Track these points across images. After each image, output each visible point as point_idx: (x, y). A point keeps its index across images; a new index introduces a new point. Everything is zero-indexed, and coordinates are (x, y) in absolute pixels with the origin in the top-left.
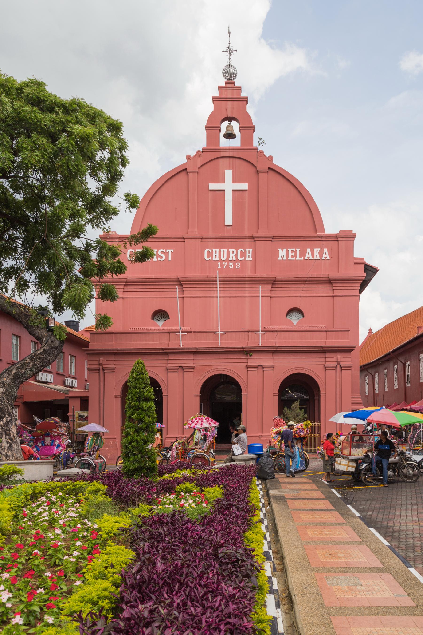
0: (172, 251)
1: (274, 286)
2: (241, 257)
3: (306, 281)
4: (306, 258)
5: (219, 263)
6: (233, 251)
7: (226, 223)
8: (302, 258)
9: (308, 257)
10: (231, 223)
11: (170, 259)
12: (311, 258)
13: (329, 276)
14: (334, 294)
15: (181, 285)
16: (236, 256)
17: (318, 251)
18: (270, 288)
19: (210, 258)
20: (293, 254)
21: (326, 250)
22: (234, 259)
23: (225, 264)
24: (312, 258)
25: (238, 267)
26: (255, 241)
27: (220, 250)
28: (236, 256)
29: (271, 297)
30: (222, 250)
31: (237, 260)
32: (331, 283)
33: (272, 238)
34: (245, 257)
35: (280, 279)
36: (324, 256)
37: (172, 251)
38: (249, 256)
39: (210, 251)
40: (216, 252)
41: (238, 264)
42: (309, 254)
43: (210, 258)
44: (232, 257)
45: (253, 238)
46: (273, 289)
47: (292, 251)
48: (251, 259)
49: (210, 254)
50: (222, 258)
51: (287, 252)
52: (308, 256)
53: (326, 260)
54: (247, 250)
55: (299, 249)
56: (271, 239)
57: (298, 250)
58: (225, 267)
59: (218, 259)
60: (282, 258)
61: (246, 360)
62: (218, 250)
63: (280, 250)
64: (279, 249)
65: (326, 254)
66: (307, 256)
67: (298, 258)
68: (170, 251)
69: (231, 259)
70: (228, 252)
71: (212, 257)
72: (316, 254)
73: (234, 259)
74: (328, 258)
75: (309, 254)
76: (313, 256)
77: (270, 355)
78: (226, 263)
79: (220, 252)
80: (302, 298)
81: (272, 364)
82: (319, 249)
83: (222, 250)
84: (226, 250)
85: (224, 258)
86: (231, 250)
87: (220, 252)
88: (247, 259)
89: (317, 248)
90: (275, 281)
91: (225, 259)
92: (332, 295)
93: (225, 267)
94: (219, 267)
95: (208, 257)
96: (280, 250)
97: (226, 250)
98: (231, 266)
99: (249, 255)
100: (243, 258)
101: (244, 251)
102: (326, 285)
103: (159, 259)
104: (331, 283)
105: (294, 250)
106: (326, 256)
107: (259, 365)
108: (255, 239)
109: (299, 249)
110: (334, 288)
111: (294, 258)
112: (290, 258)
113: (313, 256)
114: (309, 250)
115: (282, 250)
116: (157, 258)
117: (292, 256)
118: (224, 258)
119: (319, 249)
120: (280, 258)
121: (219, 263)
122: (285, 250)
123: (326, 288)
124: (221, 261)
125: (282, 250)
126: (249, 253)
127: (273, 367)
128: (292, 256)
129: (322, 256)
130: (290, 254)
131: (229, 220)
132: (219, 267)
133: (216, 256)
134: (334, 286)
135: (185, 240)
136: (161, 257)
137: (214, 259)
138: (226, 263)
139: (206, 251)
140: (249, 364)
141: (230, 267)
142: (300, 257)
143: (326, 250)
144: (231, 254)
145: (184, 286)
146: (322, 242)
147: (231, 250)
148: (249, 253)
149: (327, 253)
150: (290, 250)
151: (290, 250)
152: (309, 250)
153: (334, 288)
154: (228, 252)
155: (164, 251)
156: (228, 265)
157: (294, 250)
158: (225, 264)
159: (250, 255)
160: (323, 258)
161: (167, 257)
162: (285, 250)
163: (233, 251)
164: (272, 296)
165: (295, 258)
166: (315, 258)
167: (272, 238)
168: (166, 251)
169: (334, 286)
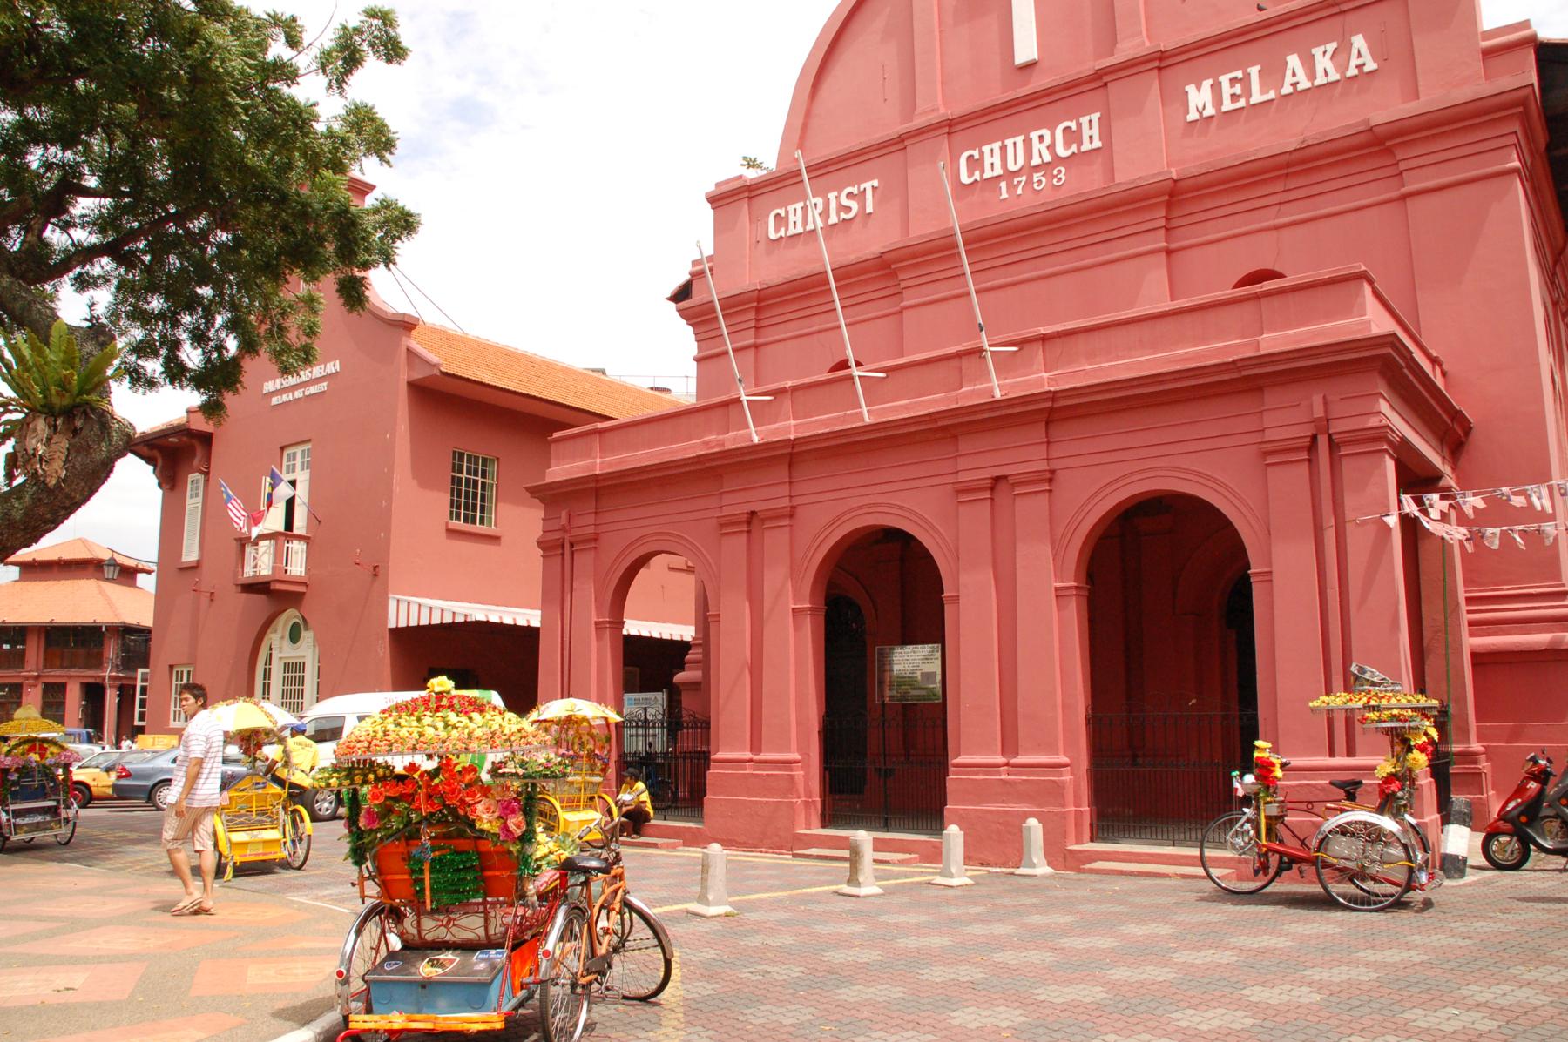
0: (875, 183)
1: (1175, 213)
2: (1067, 145)
3: (1288, 165)
4: (1287, 89)
5: (1003, 185)
6: (1041, 138)
7: (1020, 59)
8: (1272, 95)
9: (1294, 85)
10: (1035, 56)
11: (869, 209)
12: (1304, 84)
13: (1373, 124)
14: (1405, 190)
15: (894, 274)
16: (1051, 148)
17: (1329, 54)
18: (1162, 222)
19: (977, 175)
20: (1238, 89)
21: (1359, 42)
22: (1047, 158)
23: (1019, 182)
24: (1307, 85)
25: (1060, 179)
26: (1106, 84)
27: (1003, 142)
28: (1051, 148)
29: (1169, 252)
30: (1009, 142)
31: (1058, 160)
32: (1389, 151)
33: (1161, 61)
34: (1080, 144)
35: (1190, 182)
36: (1354, 62)
37: (875, 183)
38: (1092, 138)
39: (976, 154)
40: (991, 155)
41: (1059, 172)
42: (1294, 74)
43: (977, 175)
44: (1041, 154)
45: (1099, 75)
46: (1175, 223)
47: (1233, 81)
48: (1097, 144)
49: (975, 164)
50: (1012, 167)
51: (1216, 88)
52: (1294, 80)
53: (1363, 76)
54: (1084, 120)
55: (1258, 67)
56: (1156, 64)
57: (1254, 71)
58: (1019, 191)
59: (998, 171)
60: (1201, 114)
62: (996, 146)
63: (1191, 89)
64: (1187, 88)
65: (1359, 55)
66: (1289, 79)
67: (1257, 97)
68: (868, 185)
69: (1036, 161)
70: (1028, 143)
71: (982, 172)
72: (1323, 60)
73: (1047, 158)
74: (1371, 65)
75: (1294, 74)
76: (1312, 75)
77: (1038, 433)
78: (1024, 179)
79: (1003, 149)
80: (1286, 232)
81: (1043, 466)
82: (1331, 47)
83: (1009, 142)
84: (1019, 139)
85: (1015, 163)
86: (1034, 135)
87: (1003, 149)
88: (1086, 147)
89: (1325, 43)
90: (1171, 195)
91: (1021, 162)
92: (1395, 194)
93: (1019, 191)
94: (1004, 195)
95: (970, 174)
96: (1191, 89)
97: (1019, 139)
98: (1040, 182)
99: (1091, 133)
100: (1074, 148)
101: (1073, 125)
102: (1369, 164)
103: (843, 216)
104: (1389, 151)
105: (1239, 74)
106: (1360, 62)
107: (997, 479)
108: (1105, 79)
109: (1258, 67)
110: (1402, 166)
111: (1242, 103)
112: (1227, 105)
113: (1312, 75)
114: (1293, 61)
115: (1199, 88)
116: (838, 215)
117: (1234, 98)
118: (1015, 163)
119: (1331, 47)
120: (1193, 116)
121: (1003, 185)
122: (1207, 84)
123: (1371, 176)
124: (1009, 175)
125: (1199, 88)
126: (1091, 128)
127: (1051, 480)
128: (1234, 98)
129: (1347, 68)
130: (1227, 90)
131: (1026, 48)
132: (1004, 195)
133: (993, 163)
134: (1399, 157)
135: (906, 143)
136: (848, 209)
137: (988, 174)
138: (1024, 179)
139: (966, 155)
140: (963, 477)
141: (1035, 186)
142: (1263, 91)
143: (1359, 42)
144: (1036, 144)
145: (901, 277)
146: (1339, 19)
147: (1034, 135)
148: (1091, 128)
149: (1365, 51)
150: (1224, 80)
151: (1224, 80)
152: (1293, 61)
153: (1402, 166)
154: (1028, 143)
155: (856, 192)
156: (1030, 181)
157: (1239, 74)
158: (1019, 182)
159: (1095, 132)
160: (1352, 72)
161: (863, 206)
162: (1207, 84)
163: (1041, 138)
164: (1173, 246)
165: (1248, 102)
166: (1320, 80)
167: (1161, 59)
168: (859, 188)
169: (1399, 157)
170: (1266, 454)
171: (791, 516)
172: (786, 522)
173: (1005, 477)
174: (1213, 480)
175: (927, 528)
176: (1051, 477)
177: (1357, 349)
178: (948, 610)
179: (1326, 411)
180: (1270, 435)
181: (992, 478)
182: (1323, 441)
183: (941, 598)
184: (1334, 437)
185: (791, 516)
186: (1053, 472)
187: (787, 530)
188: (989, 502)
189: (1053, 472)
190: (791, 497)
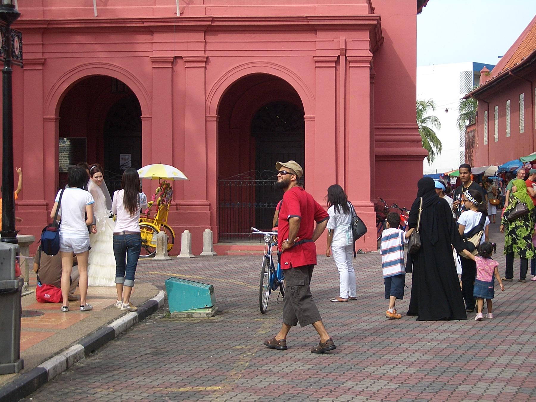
61: (150, 45)
107: (176, 58)
170: (316, 62)
171: (43, 64)
172: (40, 67)
173: (181, 58)
174: (288, 70)
175: (133, 79)
176: (207, 60)
177: (363, 20)
178: (145, 125)
179: (345, 46)
180: (319, 54)
181: (174, 57)
182: (342, 59)
183: (141, 118)
184: (348, 58)
185: (43, 64)
186: (207, 58)
187: (41, 71)
188: (171, 69)
189: (207, 58)
190: (43, 53)
